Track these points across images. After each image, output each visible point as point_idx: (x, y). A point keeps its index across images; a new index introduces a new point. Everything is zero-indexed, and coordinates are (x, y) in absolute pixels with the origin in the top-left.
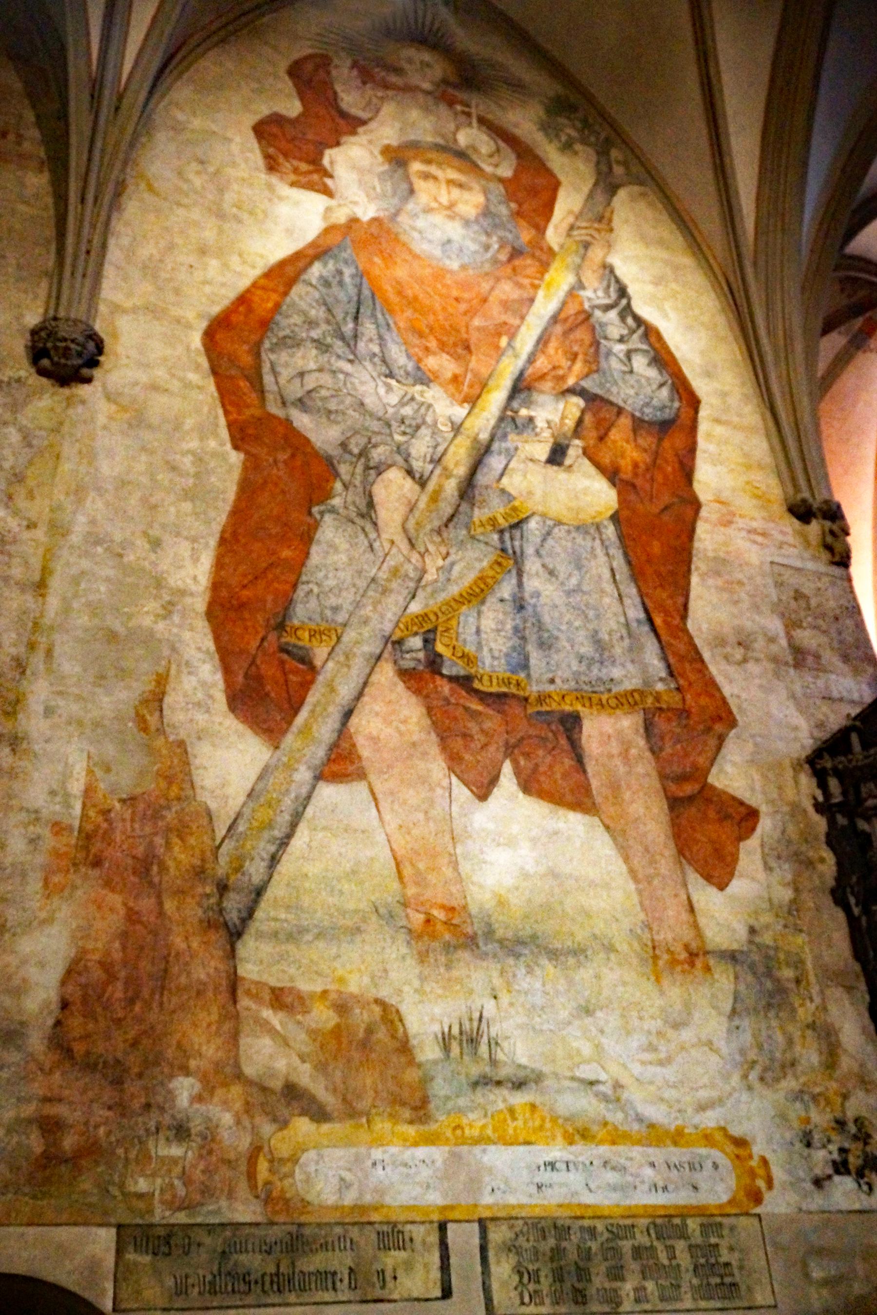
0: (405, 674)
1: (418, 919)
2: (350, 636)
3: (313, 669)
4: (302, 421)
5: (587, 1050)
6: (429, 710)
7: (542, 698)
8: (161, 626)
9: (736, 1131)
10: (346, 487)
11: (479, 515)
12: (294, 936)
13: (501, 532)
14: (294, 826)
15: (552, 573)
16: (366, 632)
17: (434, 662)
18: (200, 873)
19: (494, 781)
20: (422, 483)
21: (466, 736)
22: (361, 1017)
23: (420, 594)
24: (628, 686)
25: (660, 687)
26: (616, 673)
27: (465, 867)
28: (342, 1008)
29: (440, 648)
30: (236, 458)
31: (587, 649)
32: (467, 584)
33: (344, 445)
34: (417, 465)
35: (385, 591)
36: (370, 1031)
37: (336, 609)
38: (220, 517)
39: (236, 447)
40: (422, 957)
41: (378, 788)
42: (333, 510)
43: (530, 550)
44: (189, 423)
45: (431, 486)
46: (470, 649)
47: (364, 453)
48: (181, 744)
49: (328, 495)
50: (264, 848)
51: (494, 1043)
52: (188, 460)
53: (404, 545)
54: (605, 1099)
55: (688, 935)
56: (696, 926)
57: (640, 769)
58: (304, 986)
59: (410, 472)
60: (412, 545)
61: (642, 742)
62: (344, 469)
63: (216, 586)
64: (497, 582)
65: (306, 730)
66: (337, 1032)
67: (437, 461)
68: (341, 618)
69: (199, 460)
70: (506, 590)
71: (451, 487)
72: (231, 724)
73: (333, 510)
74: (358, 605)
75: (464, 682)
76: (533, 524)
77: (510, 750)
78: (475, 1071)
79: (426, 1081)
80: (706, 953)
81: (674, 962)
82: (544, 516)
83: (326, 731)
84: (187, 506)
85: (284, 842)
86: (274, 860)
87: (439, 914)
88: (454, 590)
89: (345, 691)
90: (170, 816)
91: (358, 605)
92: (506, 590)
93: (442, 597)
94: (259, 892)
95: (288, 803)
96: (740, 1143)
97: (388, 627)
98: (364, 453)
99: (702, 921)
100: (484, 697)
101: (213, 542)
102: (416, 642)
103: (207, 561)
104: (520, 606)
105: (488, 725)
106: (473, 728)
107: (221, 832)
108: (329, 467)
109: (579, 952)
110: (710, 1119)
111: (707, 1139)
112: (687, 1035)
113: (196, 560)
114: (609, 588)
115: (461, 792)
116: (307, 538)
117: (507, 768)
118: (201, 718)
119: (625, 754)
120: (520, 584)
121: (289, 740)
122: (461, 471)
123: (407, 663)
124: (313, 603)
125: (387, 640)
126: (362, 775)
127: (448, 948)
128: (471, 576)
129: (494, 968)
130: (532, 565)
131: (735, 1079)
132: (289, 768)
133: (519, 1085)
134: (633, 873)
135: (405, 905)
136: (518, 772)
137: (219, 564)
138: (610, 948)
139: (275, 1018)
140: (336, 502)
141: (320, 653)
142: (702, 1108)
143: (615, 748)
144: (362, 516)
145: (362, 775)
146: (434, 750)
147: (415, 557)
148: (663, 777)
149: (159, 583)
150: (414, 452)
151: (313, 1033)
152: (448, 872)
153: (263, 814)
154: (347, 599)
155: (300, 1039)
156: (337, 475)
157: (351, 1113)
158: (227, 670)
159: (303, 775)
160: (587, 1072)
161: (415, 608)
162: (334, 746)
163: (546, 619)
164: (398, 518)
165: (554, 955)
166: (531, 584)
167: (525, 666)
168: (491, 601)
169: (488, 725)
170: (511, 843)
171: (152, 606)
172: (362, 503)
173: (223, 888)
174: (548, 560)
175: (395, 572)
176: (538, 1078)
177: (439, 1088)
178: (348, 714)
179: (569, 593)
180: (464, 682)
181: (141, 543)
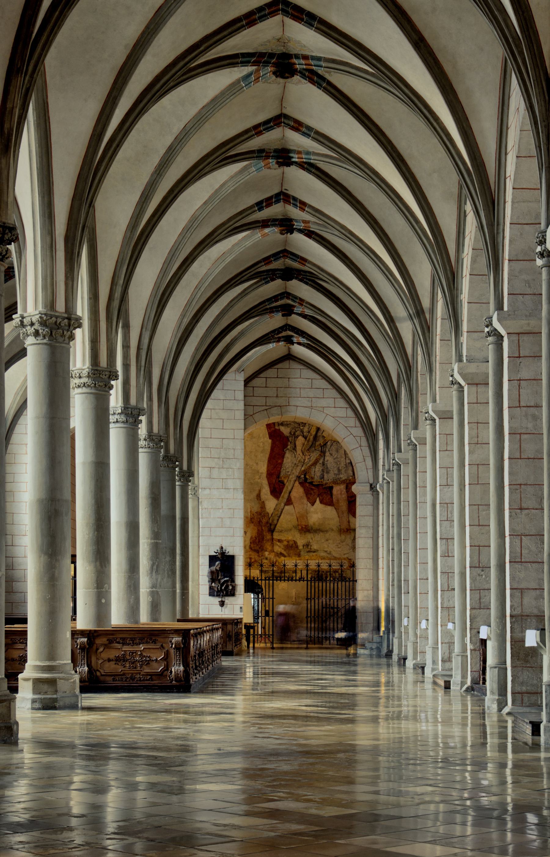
0: (300, 483)
1: (300, 527)
2: (291, 477)
3: (284, 485)
4: (282, 429)
5: (326, 546)
6: (304, 490)
7: (326, 484)
8: (259, 481)
9: (350, 558)
10: (291, 443)
11: (317, 443)
12: (281, 531)
13: (321, 447)
14: (281, 514)
15: (331, 455)
16: (293, 476)
17: (306, 479)
18: (267, 523)
19: (315, 502)
20: (305, 438)
21: (311, 494)
22: (291, 543)
23: (304, 465)
24: (344, 479)
25: (351, 478)
26: (341, 476)
27: (309, 518)
28: (288, 542)
29: (307, 477)
30: (270, 441)
31: (336, 472)
32: (313, 461)
33: (290, 433)
34: (305, 434)
35: (298, 466)
36: (292, 545)
37: (288, 472)
38: (267, 456)
39: (270, 439)
40: (301, 533)
41: (295, 505)
42: (288, 449)
43: (327, 450)
44: (261, 435)
45: (308, 439)
46: (313, 476)
47: (294, 434)
48: (263, 502)
49: (287, 446)
50: (277, 518)
51: (311, 546)
52: (261, 444)
53: (301, 454)
54: (328, 553)
55: (347, 527)
56: (349, 525)
57: (344, 496)
58: (283, 539)
59: (303, 436)
60: (303, 454)
61: (345, 490)
62: (290, 439)
63: (268, 471)
64: (320, 459)
65: (283, 497)
66: (287, 545)
67: (309, 432)
68: (289, 473)
69: (263, 443)
70: (321, 461)
71: (312, 438)
72: (271, 497)
73: (288, 449)
74: (292, 470)
75: (311, 483)
76: (329, 443)
77: (318, 496)
78: (308, 550)
79: (300, 551)
80: (350, 529)
81: (344, 531)
82: (331, 440)
83: (286, 496)
84: (262, 455)
85: (279, 517)
86: (278, 520)
87: (304, 526)
88: (311, 463)
89: (290, 488)
90: (262, 514)
91: (292, 470)
92: (321, 461)
93: (308, 465)
94: (276, 525)
95: (280, 510)
96: (350, 559)
97: (297, 474)
98: (294, 434)
99: (351, 524)
100: (315, 486)
101: (267, 461)
102: (303, 476)
103: (266, 466)
104: (323, 464)
105: (315, 491)
106: (312, 492)
107: (270, 516)
108: (287, 438)
109: (327, 531)
110: (346, 556)
111: (345, 559)
112: (344, 543)
113: (264, 466)
114: (344, 456)
115: (309, 504)
116: (283, 457)
117: (318, 499)
118: (266, 497)
119: (341, 494)
120: (324, 459)
121: (281, 499)
122: (314, 433)
123: (300, 481)
124: (284, 471)
125: (297, 476)
126: (292, 504)
127: (305, 532)
128: (315, 459)
129: (312, 535)
130: (327, 454)
131: (351, 550)
132: (280, 504)
133: (314, 552)
134: (339, 516)
135: (298, 525)
136: (320, 499)
137: (268, 466)
138: (333, 530)
139: (279, 544)
140: (289, 447)
141: (285, 481)
142: (344, 555)
143: (339, 492)
144: (293, 449)
145: (292, 504)
146: (305, 497)
147: (304, 457)
148: (348, 497)
149: (258, 472)
150: (304, 431)
151: (284, 546)
152: (306, 519)
153: (276, 513)
154: (290, 470)
155: (282, 546)
156: (289, 440)
157: (289, 556)
158: (270, 487)
159: (283, 505)
160: (326, 550)
161: (303, 469)
162: (288, 499)
163: (329, 466)
164: (300, 448)
165: (322, 531)
166: (326, 458)
167: (323, 478)
168: (318, 464)
169: (315, 491)
170: (317, 513)
171: (257, 477)
172: (293, 446)
173: (271, 525)
174: (331, 452)
175: (299, 461)
176: (318, 551)
177: (302, 553)
178: (290, 492)
179: (334, 459)
180: (311, 483)
181: (255, 465)
